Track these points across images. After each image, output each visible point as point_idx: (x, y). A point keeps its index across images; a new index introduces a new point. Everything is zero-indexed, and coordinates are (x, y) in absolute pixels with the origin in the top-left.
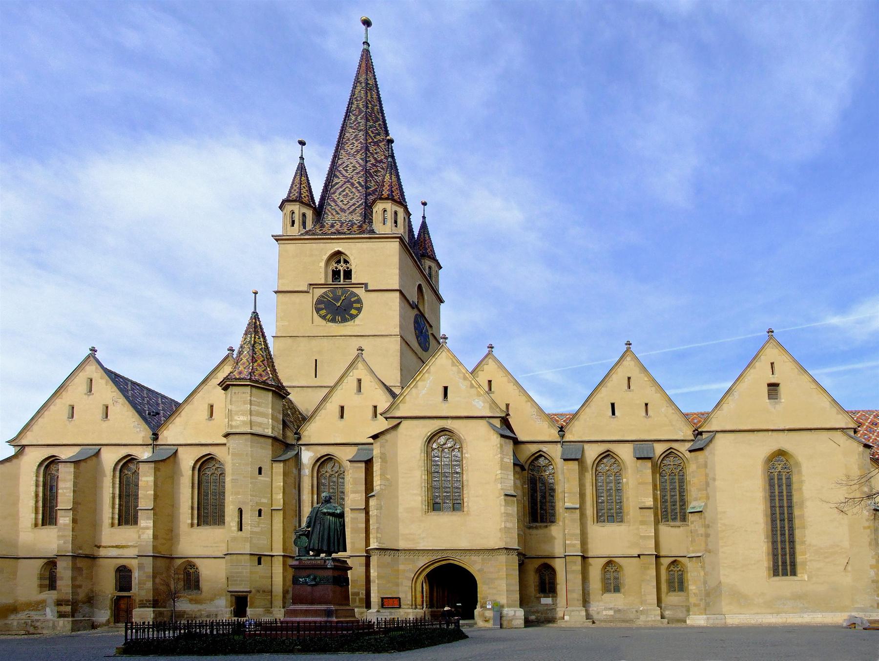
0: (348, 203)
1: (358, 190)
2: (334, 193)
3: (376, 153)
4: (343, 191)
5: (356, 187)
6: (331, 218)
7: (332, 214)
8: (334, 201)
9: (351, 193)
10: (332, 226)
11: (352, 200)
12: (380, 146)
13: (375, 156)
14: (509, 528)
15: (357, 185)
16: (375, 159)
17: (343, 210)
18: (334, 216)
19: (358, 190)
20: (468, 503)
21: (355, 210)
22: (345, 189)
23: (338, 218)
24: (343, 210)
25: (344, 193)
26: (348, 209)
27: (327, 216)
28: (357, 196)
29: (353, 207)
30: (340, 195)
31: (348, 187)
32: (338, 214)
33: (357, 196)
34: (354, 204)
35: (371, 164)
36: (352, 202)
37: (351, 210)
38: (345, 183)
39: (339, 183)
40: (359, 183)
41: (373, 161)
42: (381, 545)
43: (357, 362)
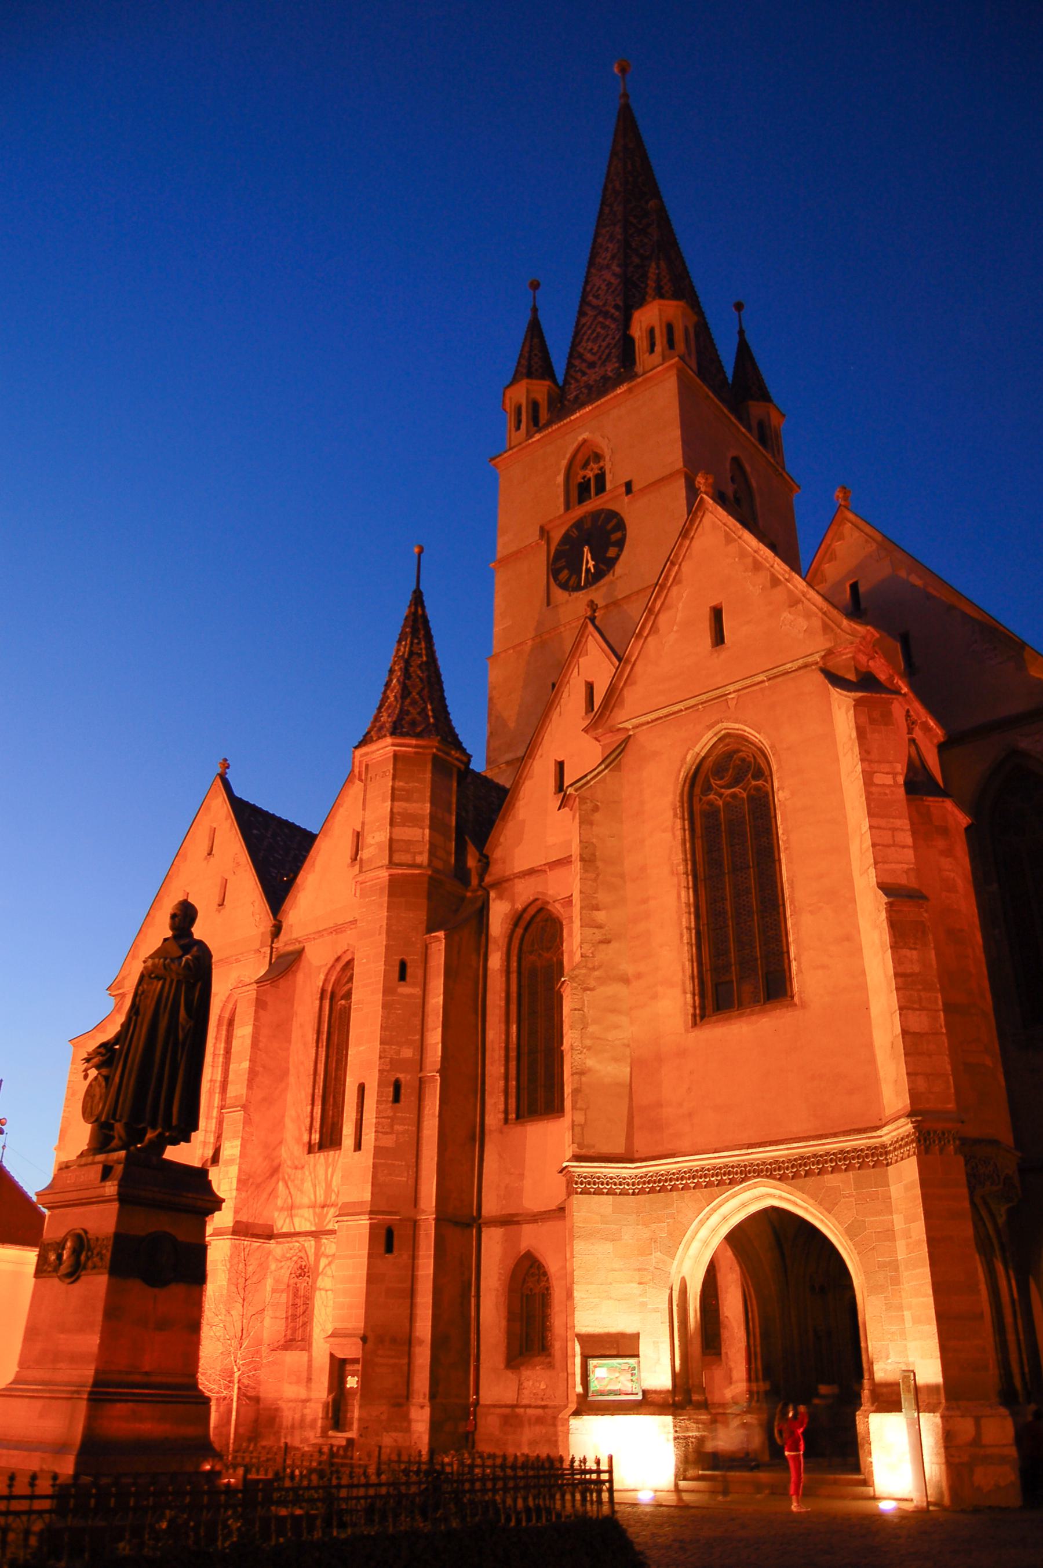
2: (580, 343)
7: (577, 381)
8: (581, 356)
11: (604, 340)
13: (642, 251)
14: (915, 1034)
15: (613, 311)
17: (592, 365)
21: (609, 355)
26: (600, 358)
29: (607, 351)
31: (600, 322)
34: (607, 347)
36: (604, 344)
37: (604, 357)
38: (596, 316)
40: (616, 307)
41: (637, 260)
43: (584, 640)
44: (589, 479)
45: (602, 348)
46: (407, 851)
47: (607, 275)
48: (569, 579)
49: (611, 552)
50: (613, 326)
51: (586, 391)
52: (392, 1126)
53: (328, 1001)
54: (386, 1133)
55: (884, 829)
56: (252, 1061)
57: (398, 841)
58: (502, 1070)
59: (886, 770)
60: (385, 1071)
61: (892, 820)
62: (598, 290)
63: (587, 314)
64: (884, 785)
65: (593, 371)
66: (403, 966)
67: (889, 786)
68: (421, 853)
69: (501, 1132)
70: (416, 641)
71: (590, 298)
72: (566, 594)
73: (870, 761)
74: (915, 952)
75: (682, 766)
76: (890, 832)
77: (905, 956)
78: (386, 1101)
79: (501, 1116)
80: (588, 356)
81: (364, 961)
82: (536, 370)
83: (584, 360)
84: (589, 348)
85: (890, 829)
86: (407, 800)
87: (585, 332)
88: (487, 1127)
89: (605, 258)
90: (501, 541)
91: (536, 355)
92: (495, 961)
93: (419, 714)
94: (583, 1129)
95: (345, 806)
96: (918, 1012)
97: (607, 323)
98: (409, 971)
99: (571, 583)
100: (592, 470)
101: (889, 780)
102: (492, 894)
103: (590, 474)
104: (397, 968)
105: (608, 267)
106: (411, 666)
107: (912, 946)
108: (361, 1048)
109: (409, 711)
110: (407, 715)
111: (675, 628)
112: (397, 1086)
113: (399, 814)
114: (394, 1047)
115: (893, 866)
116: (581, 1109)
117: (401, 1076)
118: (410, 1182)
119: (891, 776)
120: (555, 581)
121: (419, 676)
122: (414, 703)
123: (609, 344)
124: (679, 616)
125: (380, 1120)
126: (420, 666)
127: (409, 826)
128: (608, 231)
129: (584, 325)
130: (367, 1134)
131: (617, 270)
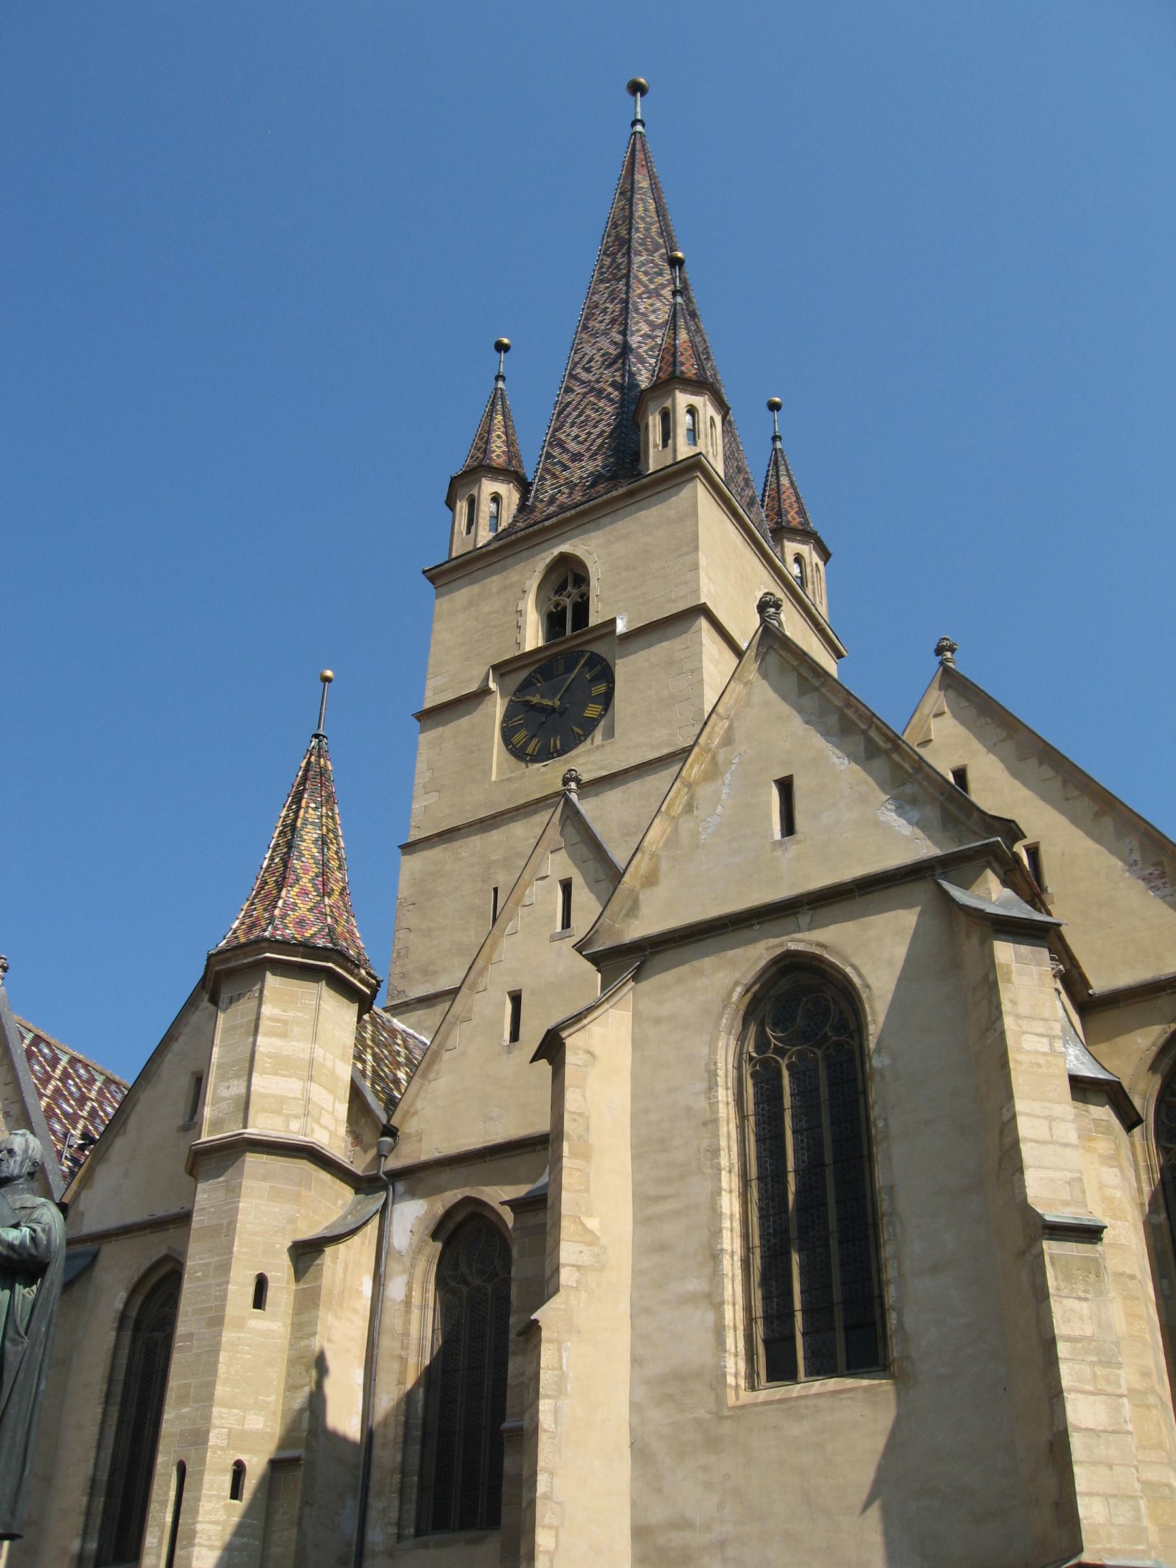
0: (588, 437)
1: (611, 400)
3: (654, 311)
4: (579, 415)
5: (610, 394)
6: (553, 484)
7: (554, 476)
8: (561, 444)
9: (597, 411)
10: (552, 500)
11: (595, 426)
12: (662, 296)
13: (652, 317)
15: (610, 390)
16: (650, 324)
17: (577, 457)
18: (558, 478)
19: (611, 400)
20: (900, 1316)
22: (585, 408)
23: (567, 478)
24: (577, 457)
25: (582, 418)
26: (588, 449)
27: (543, 484)
28: (608, 413)
29: (599, 441)
30: (572, 426)
32: (566, 468)
33: (608, 413)
34: (599, 436)
35: (640, 336)
36: (597, 431)
38: (585, 395)
39: (573, 400)
40: (613, 384)
41: (645, 329)
44: (564, 609)
45: (593, 437)
46: (279, 1112)
47: (604, 343)
48: (526, 744)
49: (592, 711)
50: (609, 409)
51: (567, 491)
53: (129, 1333)
55: (1037, 1117)
57: (265, 1096)
58: (399, 1458)
59: (1038, 1031)
60: (221, 1448)
61: (1049, 1105)
62: (590, 361)
63: (573, 391)
64: (1036, 1052)
65: (577, 464)
66: (261, 1284)
67: (1044, 1054)
68: (297, 1117)
69: (391, 1555)
70: (313, 805)
71: (579, 370)
72: (523, 765)
74: (1084, 1304)
76: (1046, 1123)
77: (1073, 1310)
78: (219, 1497)
79: (393, 1530)
80: (572, 446)
81: (200, 1274)
82: (498, 456)
83: (566, 450)
84: (573, 434)
85: (1045, 1118)
86: (284, 1035)
87: (567, 416)
88: (368, 1547)
89: (601, 322)
90: (431, 684)
91: (499, 437)
92: (396, 1288)
93: (308, 910)
94: (551, 1561)
95: (182, 1039)
96: (1091, 1398)
97: (601, 404)
98: (270, 1294)
99: (529, 750)
100: (569, 597)
103: (568, 602)
104: (251, 1290)
105: (606, 333)
106: (304, 841)
107: (1082, 1295)
108: (184, 1410)
109: (295, 904)
110: (293, 910)
111: (719, 809)
113: (269, 1055)
114: (235, 1411)
115: (1050, 1174)
116: (550, 1527)
117: (244, 1458)
119: (1045, 1040)
120: (507, 745)
121: (313, 857)
122: (304, 892)
123: (604, 431)
124: (725, 790)
125: (210, 1526)
126: (315, 842)
128: (607, 288)
129: (570, 403)
130: (183, 1548)
131: (619, 338)
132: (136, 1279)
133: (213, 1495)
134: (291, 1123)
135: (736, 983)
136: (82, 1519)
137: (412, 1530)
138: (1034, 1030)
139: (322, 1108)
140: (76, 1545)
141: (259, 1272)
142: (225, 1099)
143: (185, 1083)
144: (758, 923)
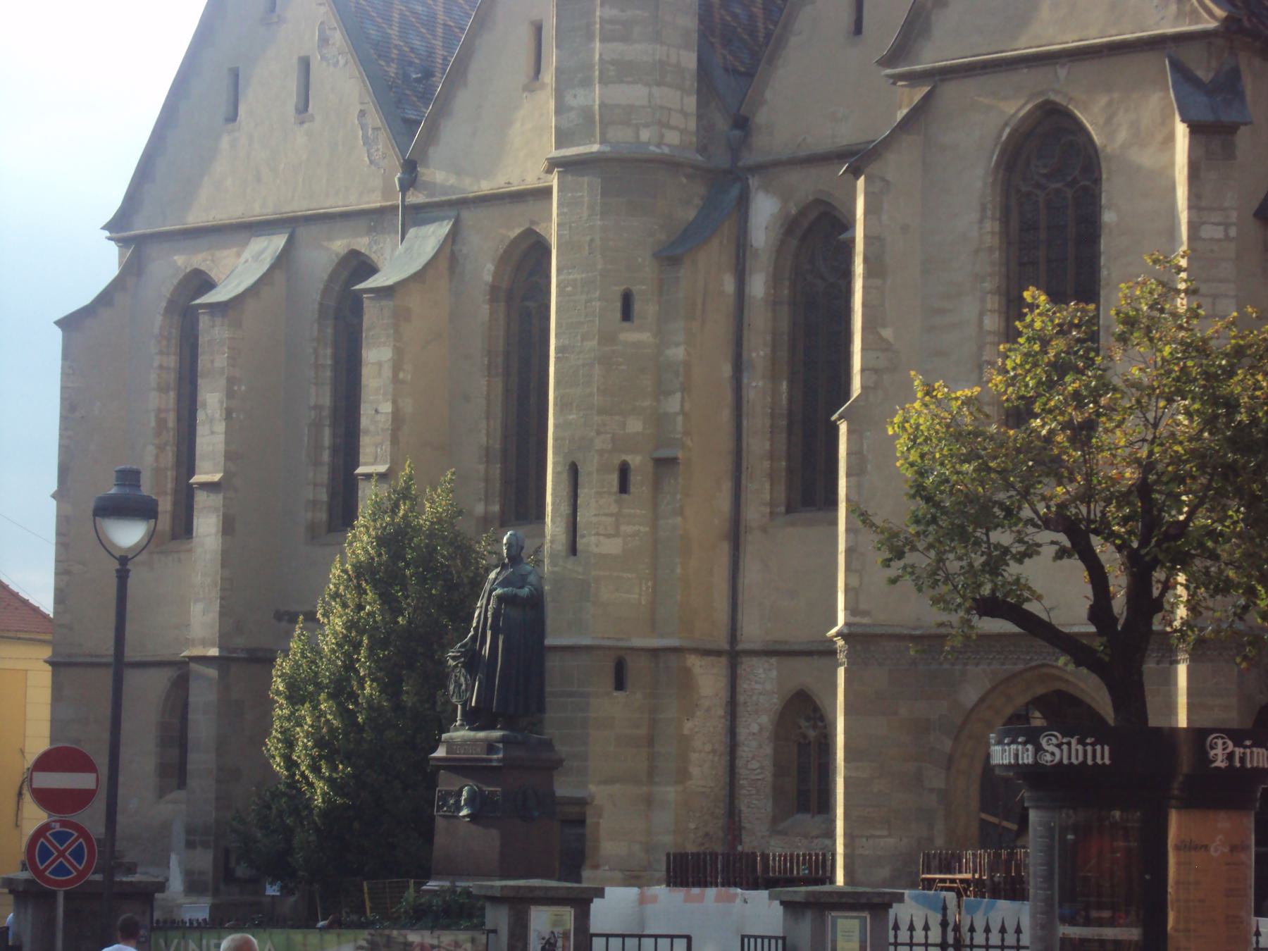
42: (858, 619)
52: (617, 528)
54: (608, 536)
56: (394, 402)
58: (767, 446)
64: (1212, 239)
67: (1219, 240)
68: (646, 126)
69: (764, 530)
73: (1200, 209)
75: (996, 145)
86: (625, 38)
92: (758, 286)
101: (1218, 233)
102: (753, 182)
104: (619, 305)
108: (571, 417)
112: (624, 472)
114: (617, 418)
117: (629, 458)
118: (643, 602)
119: (1221, 228)
125: (603, 518)
127: (628, 83)
132: (502, 251)
133: (604, 492)
134: (641, 132)
135: (1006, 124)
136: (482, 485)
137: (783, 509)
138: (1212, 220)
139: (670, 110)
140: (480, 509)
141: (623, 288)
142: (572, 108)
143: (524, 34)
144: (1026, 67)
